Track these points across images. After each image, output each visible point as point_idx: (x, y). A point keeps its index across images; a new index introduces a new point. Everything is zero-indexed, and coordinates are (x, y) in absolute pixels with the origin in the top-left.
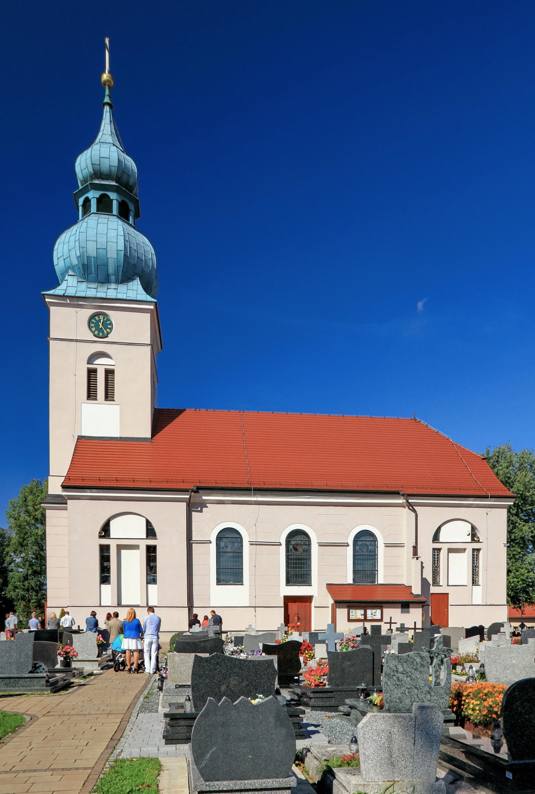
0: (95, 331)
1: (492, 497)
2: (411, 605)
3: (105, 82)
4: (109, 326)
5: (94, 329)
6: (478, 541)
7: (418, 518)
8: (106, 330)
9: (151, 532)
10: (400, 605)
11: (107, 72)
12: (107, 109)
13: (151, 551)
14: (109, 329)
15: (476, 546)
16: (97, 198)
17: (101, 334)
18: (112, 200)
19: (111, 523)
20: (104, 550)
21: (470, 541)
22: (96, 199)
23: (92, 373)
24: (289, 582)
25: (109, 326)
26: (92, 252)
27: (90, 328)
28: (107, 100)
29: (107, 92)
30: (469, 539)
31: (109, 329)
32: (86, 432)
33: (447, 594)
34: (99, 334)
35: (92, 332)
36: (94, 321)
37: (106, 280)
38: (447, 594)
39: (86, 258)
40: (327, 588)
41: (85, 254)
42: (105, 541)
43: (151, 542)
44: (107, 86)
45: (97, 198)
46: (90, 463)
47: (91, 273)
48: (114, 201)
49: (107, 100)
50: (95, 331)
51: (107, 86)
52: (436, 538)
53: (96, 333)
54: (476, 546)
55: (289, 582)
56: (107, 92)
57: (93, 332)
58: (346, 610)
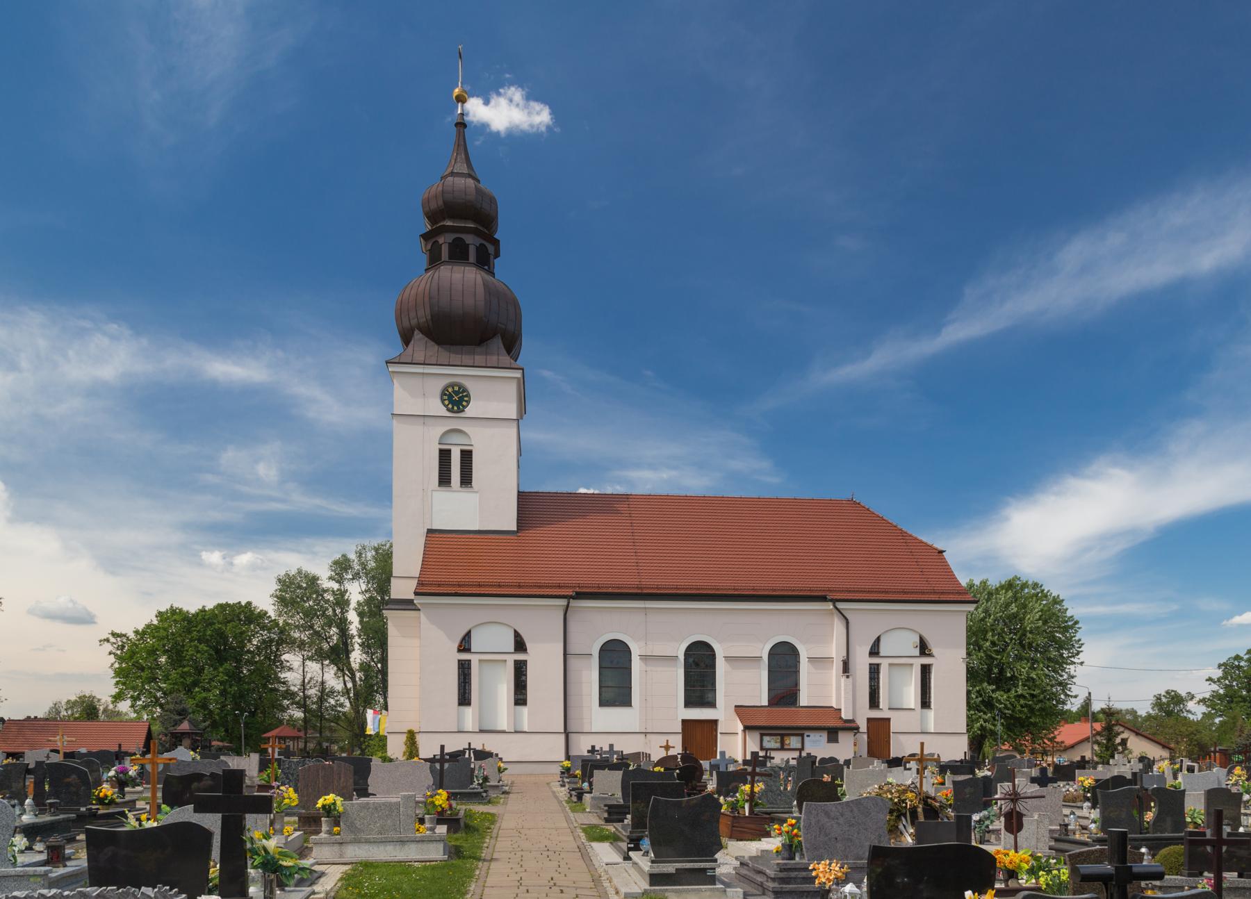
0: (448, 405)
4: (466, 399)
5: (447, 402)
6: (930, 655)
7: (850, 624)
9: (520, 646)
14: (466, 401)
15: (926, 661)
16: (449, 243)
17: (455, 408)
18: (468, 244)
21: (918, 654)
22: (447, 244)
23: (445, 455)
24: (689, 703)
25: (466, 399)
27: (443, 401)
30: (917, 652)
31: (466, 401)
33: (889, 720)
34: (453, 408)
38: (889, 720)
40: (735, 710)
43: (520, 657)
46: (446, 564)
48: (470, 246)
50: (448, 405)
53: (450, 406)
54: (926, 661)
55: (689, 703)
57: (446, 406)
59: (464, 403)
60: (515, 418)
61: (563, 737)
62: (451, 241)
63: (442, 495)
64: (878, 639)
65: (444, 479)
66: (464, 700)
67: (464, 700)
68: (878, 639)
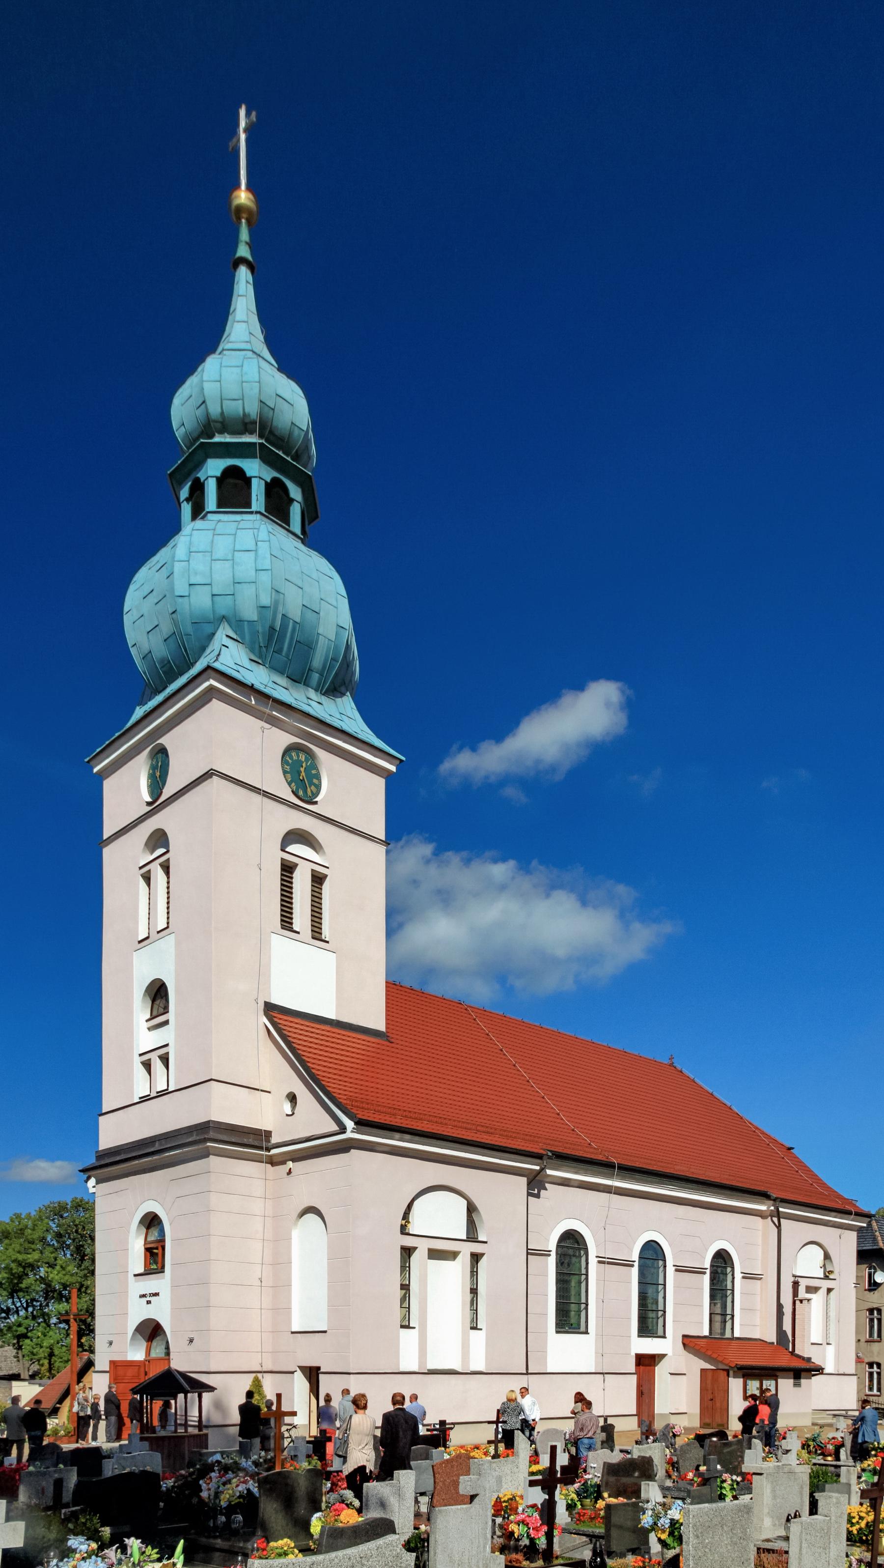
2: (803, 1374)
3: (240, 209)
8: (310, 787)
10: (792, 1374)
11: (243, 186)
12: (243, 275)
16: (266, 482)
22: (263, 483)
26: (294, 610)
28: (243, 251)
29: (244, 234)
36: (290, 761)
37: (300, 678)
39: (279, 617)
41: (280, 608)
44: (243, 221)
45: (266, 482)
47: (279, 651)
49: (243, 251)
51: (243, 221)
56: (244, 234)
58: (741, 1380)
62: (269, 480)
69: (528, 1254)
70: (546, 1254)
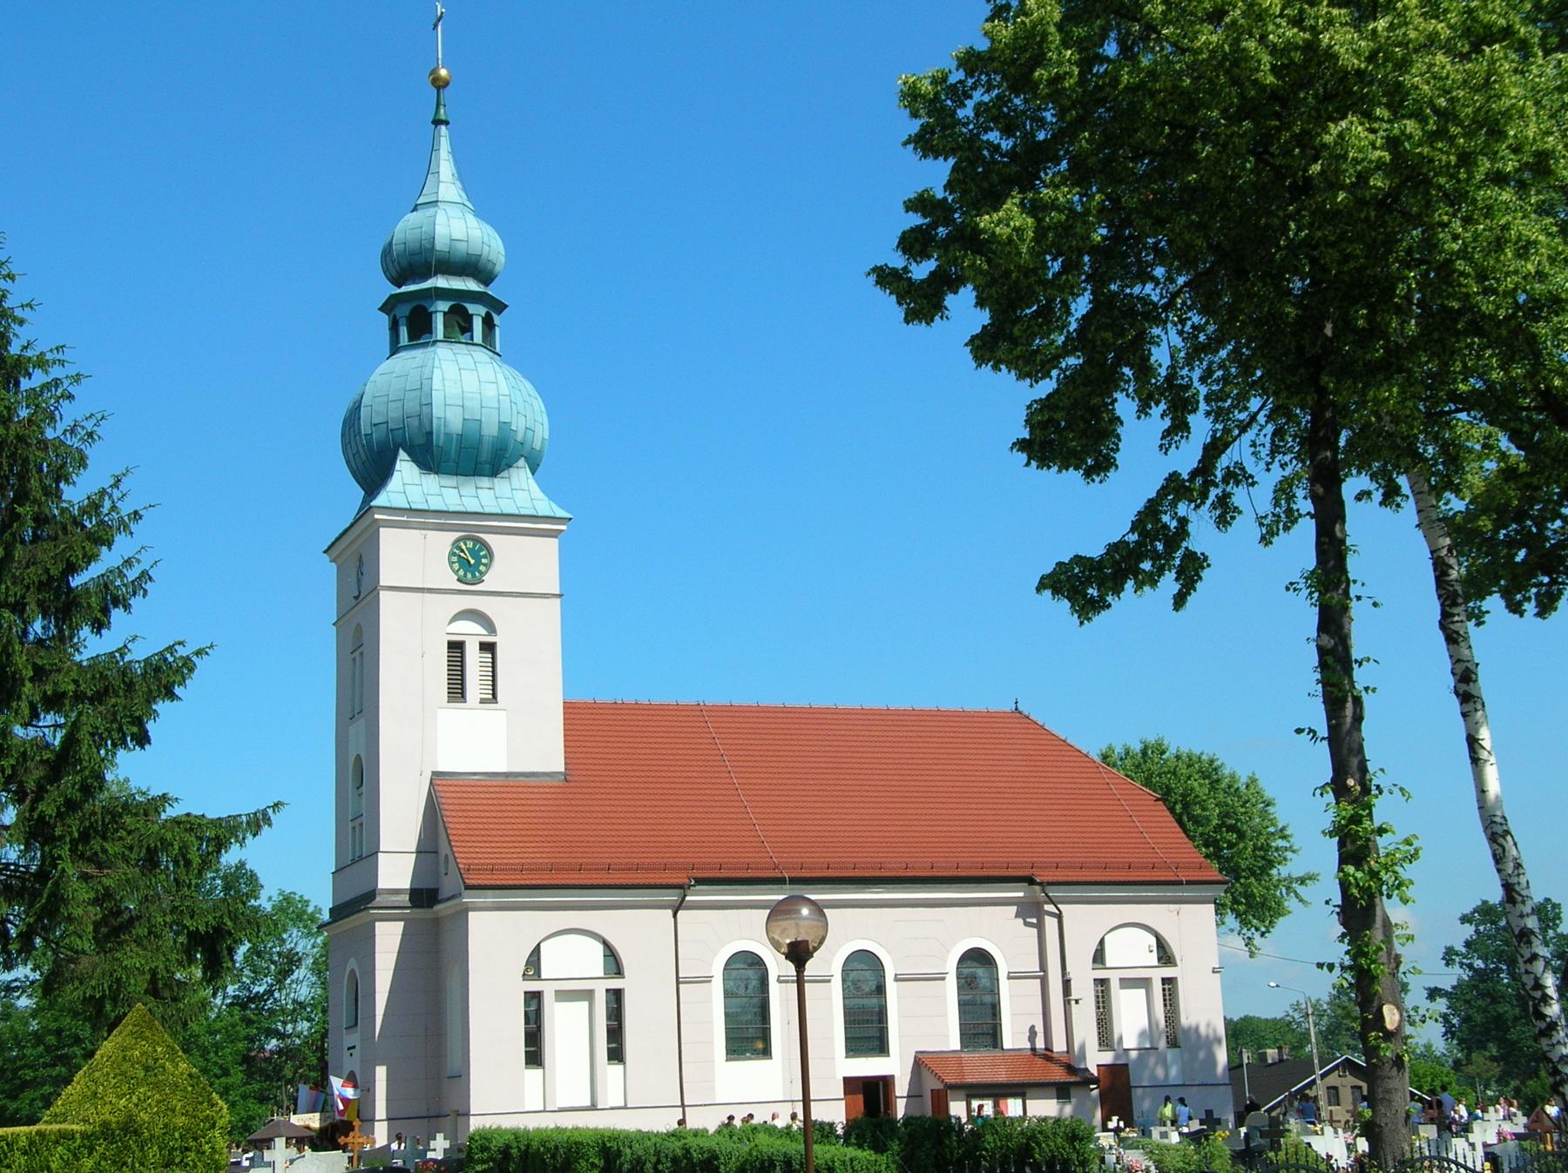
1: (1189, 883)
5: (456, 566)
13: (616, 996)
14: (485, 565)
17: (469, 575)
19: (542, 945)
20: (534, 1000)
27: (451, 563)
31: (485, 565)
32: (443, 767)
34: (465, 575)
35: (453, 571)
42: (534, 986)
43: (615, 984)
52: (1099, 957)
53: (461, 572)
57: (456, 572)
59: (482, 568)
60: (558, 593)
61: (681, 1109)
63: (454, 715)
64: (1102, 942)
65: (457, 690)
66: (534, 1058)
67: (534, 1058)
68: (1102, 942)
69: (678, 983)
70: (707, 980)
